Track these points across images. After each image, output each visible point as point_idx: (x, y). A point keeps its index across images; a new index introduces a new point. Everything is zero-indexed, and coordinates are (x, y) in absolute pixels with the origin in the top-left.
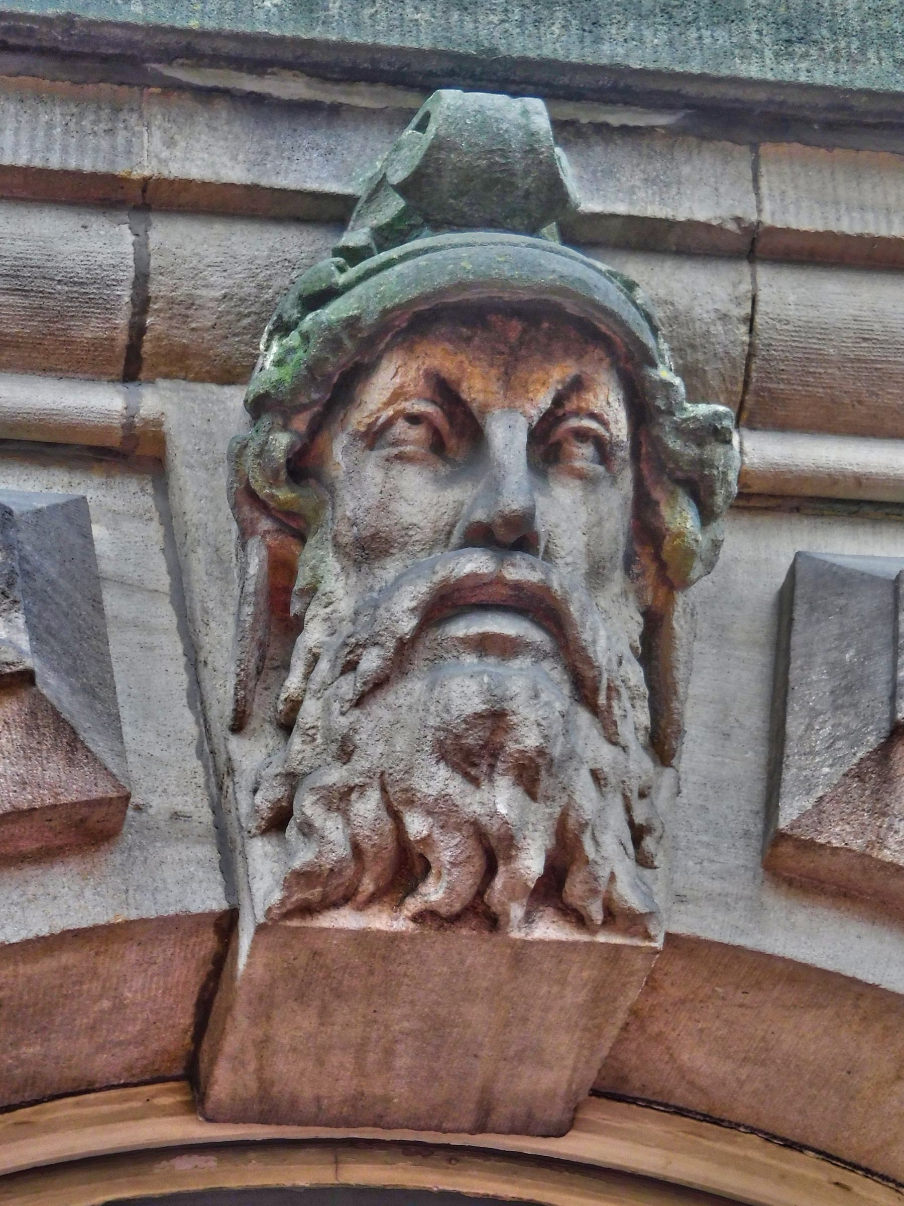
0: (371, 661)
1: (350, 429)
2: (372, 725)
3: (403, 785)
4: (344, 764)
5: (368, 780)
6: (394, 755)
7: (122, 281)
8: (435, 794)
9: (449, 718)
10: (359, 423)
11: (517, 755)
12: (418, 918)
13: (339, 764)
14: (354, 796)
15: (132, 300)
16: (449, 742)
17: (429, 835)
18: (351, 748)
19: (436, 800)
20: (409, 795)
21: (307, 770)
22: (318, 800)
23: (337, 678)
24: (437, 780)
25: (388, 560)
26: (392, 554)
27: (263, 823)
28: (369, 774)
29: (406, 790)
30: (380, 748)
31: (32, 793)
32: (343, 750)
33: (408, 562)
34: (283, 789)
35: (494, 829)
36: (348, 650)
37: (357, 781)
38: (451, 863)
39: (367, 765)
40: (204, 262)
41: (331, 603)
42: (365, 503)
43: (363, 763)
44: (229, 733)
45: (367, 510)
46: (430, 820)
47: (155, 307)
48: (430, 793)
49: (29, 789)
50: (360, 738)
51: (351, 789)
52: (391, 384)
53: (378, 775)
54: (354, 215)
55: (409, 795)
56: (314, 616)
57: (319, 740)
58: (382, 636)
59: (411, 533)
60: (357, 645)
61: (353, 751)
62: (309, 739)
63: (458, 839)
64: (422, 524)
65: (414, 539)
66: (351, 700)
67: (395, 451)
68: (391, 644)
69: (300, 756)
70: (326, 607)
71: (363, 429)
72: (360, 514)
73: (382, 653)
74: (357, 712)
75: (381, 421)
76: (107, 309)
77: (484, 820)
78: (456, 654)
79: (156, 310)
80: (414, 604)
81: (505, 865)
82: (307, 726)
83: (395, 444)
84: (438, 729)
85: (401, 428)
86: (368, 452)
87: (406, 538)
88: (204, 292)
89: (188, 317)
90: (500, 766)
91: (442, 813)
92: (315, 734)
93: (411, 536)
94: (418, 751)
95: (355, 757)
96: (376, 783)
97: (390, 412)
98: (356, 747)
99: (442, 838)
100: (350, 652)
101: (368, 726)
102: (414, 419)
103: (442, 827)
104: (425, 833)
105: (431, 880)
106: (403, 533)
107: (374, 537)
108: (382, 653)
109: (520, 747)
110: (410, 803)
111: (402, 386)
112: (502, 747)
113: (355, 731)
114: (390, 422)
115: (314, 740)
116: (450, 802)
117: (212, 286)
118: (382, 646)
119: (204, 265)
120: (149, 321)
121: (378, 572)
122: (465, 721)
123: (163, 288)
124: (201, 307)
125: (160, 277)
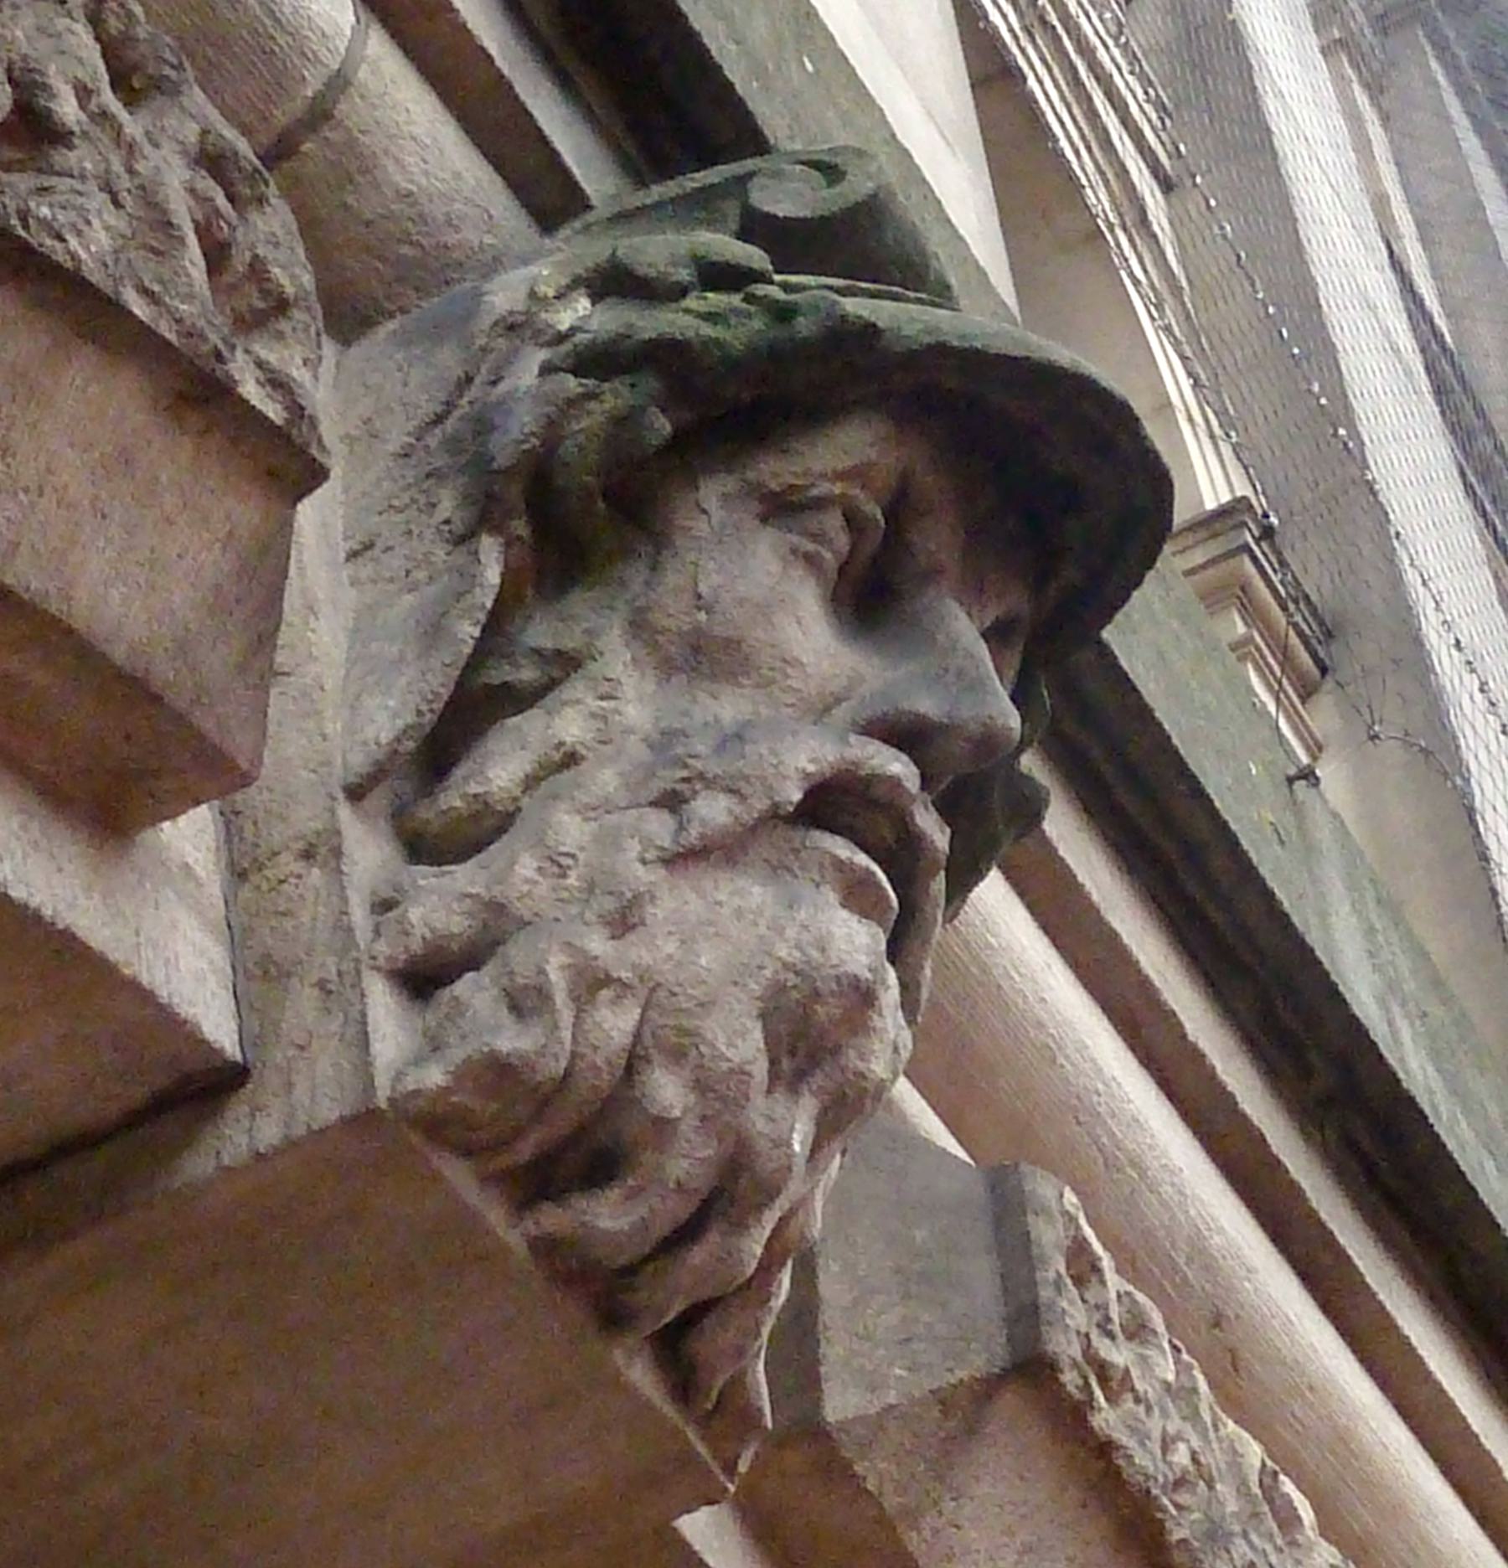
0: (713, 811)
1: (751, 475)
2: (673, 905)
3: (685, 1023)
4: (613, 938)
5: (636, 982)
6: (692, 967)
7: (321, 62)
8: (737, 1060)
9: (821, 960)
10: (775, 475)
11: (851, 1077)
12: (546, 1248)
13: (607, 932)
14: (605, 994)
15: (314, 98)
16: (795, 995)
17: (678, 1119)
18: (636, 920)
19: (731, 1070)
20: (686, 1041)
21: (527, 916)
22: (569, 966)
23: (639, 805)
24: (741, 1043)
25: (728, 689)
26: (741, 686)
27: (403, 957)
28: (643, 974)
29: (682, 1031)
30: (671, 947)
31: (177, 672)
32: (624, 916)
33: (764, 711)
34: (467, 923)
35: (772, 1165)
36: (685, 773)
37: (624, 975)
38: (679, 1183)
39: (647, 958)
40: (411, 128)
41: (615, 698)
42: (742, 588)
43: (643, 953)
44: (341, 796)
45: (741, 602)
46: (692, 1098)
47: (328, 134)
48: (729, 1055)
49: (178, 664)
50: (656, 913)
51: (607, 981)
52: (843, 454)
53: (651, 984)
54: (577, 224)
55: (686, 1041)
56: (578, 702)
57: (572, 880)
58: (748, 782)
59: (789, 670)
60: (701, 776)
61: (634, 926)
62: (556, 870)
63: (711, 1152)
64: (809, 670)
65: (789, 682)
66: (662, 849)
67: (811, 547)
68: (760, 805)
69: (526, 888)
70: (602, 698)
71: (774, 486)
72: (726, 597)
73: (738, 809)
74: (662, 872)
75: (815, 492)
76: (279, 84)
77: (762, 1145)
78: (817, 878)
79: (326, 139)
80: (811, 768)
81: (723, 1234)
82: (563, 849)
83: (815, 537)
84: (786, 966)
85: (833, 521)
86: (757, 522)
87: (778, 676)
88: (391, 168)
89: (351, 182)
90: (818, 1079)
91: (722, 1099)
92: (569, 867)
93: (787, 676)
94: (736, 983)
95: (631, 937)
96: (643, 993)
97: (837, 489)
98: (643, 923)
99: (692, 1136)
100: (684, 780)
101: (676, 901)
102: (853, 520)
103: (704, 1118)
104: (677, 1113)
105: (614, 1194)
106: (778, 664)
107: (732, 645)
108: (738, 809)
109: (861, 1066)
110: (677, 1055)
111: (870, 465)
112: (836, 1051)
113: (653, 898)
114: (820, 504)
115: (564, 876)
116: (743, 1087)
117: (403, 167)
118: (743, 798)
119: (410, 132)
120: (307, 147)
121: (702, 696)
122: (838, 978)
123: (355, 119)
124: (377, 186)
125: (358, 100)
